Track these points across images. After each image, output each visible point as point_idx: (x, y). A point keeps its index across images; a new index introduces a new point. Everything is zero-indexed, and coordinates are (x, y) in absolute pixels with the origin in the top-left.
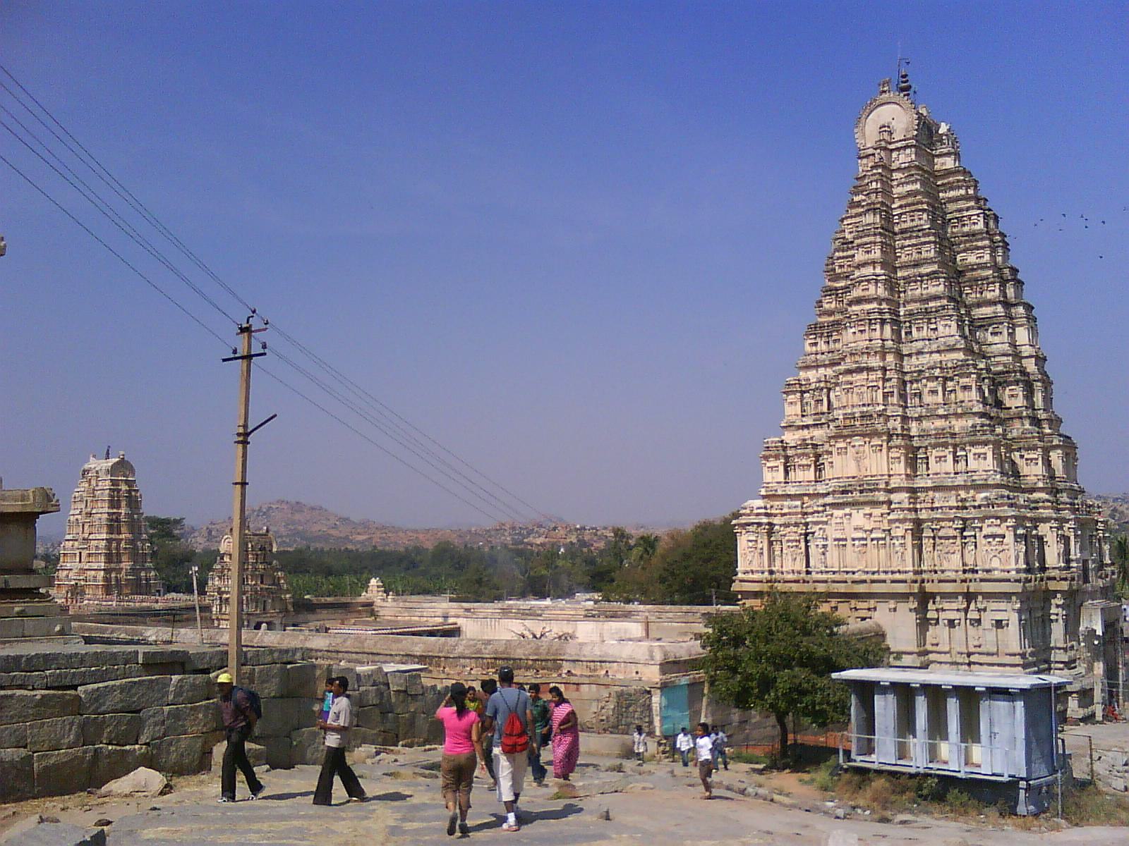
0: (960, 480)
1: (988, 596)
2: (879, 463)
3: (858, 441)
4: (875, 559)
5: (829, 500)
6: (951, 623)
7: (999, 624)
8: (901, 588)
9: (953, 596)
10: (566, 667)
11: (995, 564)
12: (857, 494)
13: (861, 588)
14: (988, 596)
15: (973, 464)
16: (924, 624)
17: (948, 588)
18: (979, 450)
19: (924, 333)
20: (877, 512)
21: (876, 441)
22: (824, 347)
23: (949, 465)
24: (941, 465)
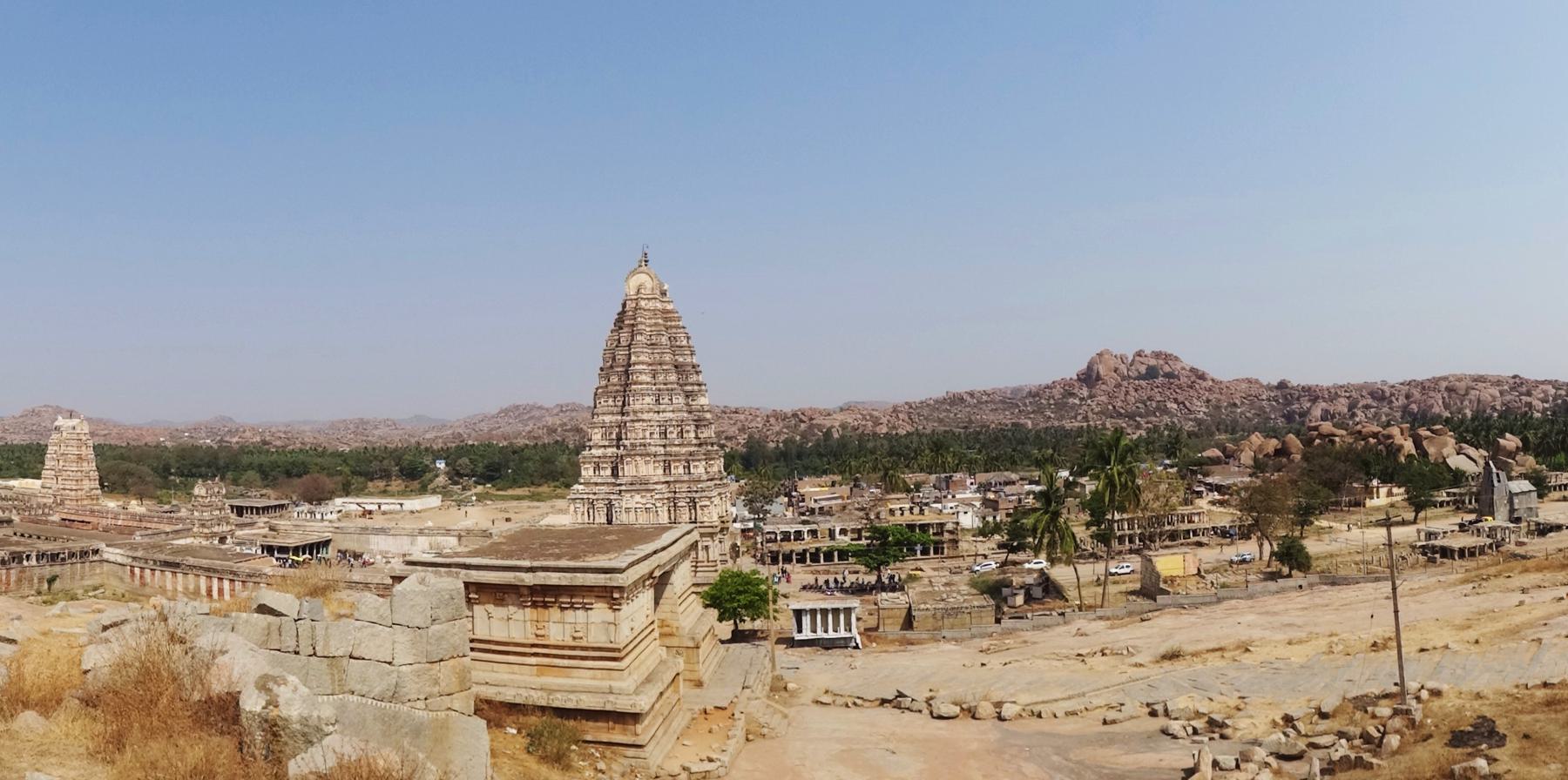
12: (640, 486)
24: (678, 470)
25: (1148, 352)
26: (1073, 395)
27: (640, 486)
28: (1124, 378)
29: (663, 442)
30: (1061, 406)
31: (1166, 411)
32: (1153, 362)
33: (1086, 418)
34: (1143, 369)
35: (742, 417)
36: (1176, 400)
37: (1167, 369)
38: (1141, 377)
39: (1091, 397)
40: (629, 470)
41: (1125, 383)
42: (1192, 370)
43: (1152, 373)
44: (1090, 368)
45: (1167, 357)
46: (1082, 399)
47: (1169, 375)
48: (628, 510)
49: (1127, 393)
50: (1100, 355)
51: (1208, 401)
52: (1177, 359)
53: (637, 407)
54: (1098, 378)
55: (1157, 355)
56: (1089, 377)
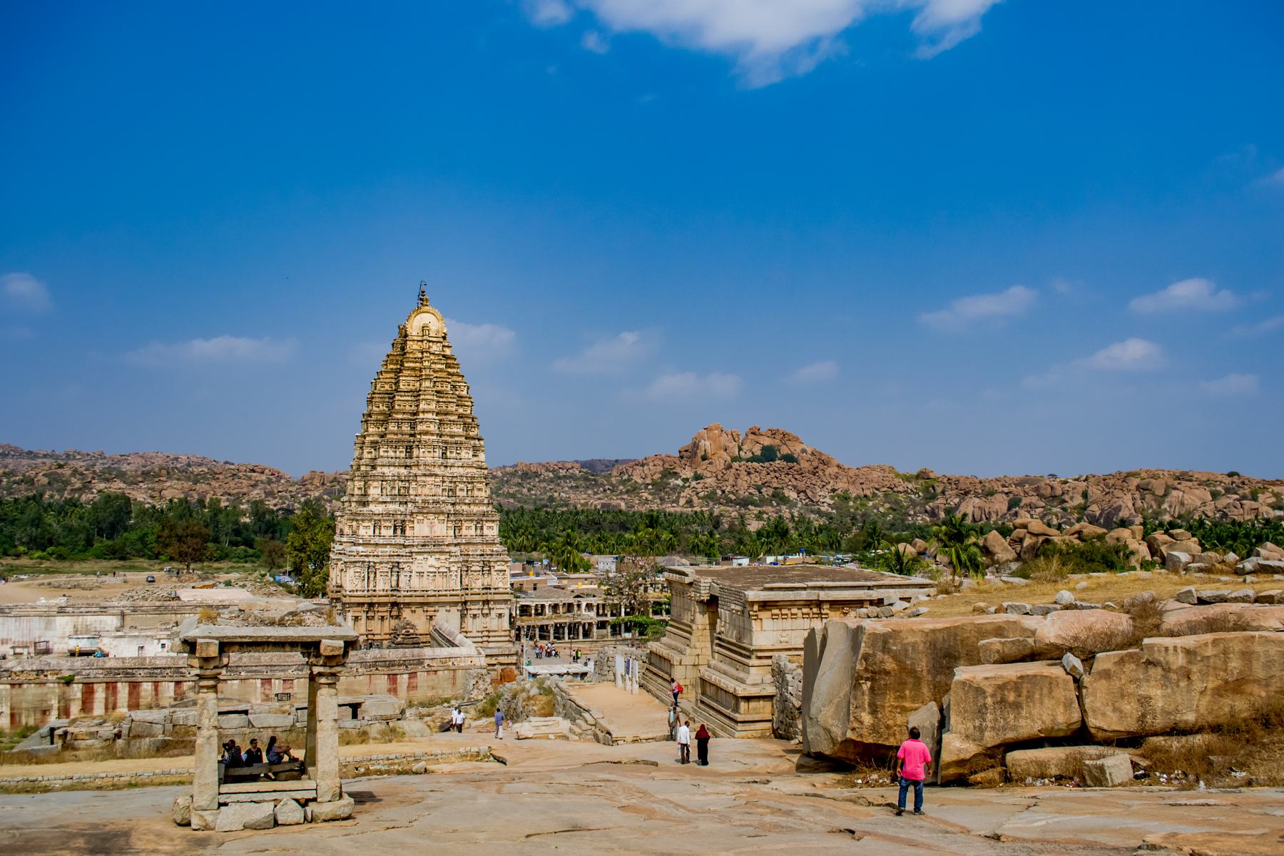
0: (479, 540)
1: (496, 602)
2: (442, 529)
3: (431, 517)
4: (440, 583)
5: (415, 549)
6: (475, 616)
7: (500, 615)
9: (477, 602)
10: (427, 662)
11: (500, 585)
13: (432, 600)
14: (496, 602)
15: (486, 531)
16: (463, 616)
17: (477, 597)
18: (490, 524)
19: (454, 455)
20: (443, 557)
21: (442, 517)
22: (391, 454)
23: (472, 532)
24: (469, 531)
26: (676, 475)
27: (432, 546)
28: (734, 459)
29: (452, 500)
30: (659, 487)
31: (783, 500)
32: (767, 442)
33: (690, 502)
35: (264, 477)
37: (785, 450)
39: (698, 477)
40: (420, 529)
41: (736, 465)
43: (768, 454)
44: (696, 445)
46: (685, 480)
47: (789, 458)
48: (420, 574)
52: (796, 439)
53: (429, 460)
55: (774, 434)
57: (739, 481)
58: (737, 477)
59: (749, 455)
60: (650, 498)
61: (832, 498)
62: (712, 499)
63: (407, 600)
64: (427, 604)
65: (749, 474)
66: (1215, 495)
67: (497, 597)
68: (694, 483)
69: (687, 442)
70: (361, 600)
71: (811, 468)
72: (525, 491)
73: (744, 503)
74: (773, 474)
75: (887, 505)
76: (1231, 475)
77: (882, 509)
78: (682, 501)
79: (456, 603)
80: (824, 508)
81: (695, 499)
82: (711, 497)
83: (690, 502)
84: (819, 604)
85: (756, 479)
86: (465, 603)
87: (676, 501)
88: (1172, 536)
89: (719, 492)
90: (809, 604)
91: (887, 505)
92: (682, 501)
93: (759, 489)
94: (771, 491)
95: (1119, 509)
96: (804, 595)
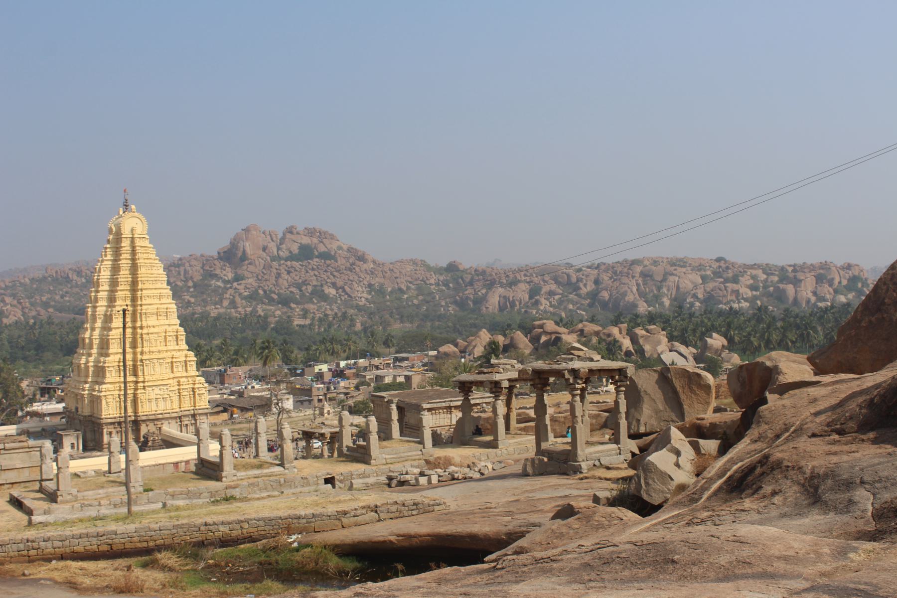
8: (175, 415)
13: (160, 416)
17: (187, 413)
25: (300, 228)
28: (273, 259)
31: (324, 297)
32: (306, 240)
33: (233, 304)
34: (295, 249)
36: (334, 285)
37: (322, 248)
38: (292, 257)
41: (275, 264)
42: (350, 250)
43: (306, 253)
44: (234, 245)
45: (323, 235)
46: (226, 282)
48: (150, 400)
49: (278, 276)
50: (247, 230)
51: (370, 285)
52: (332, 237)
54: (244, 257)
55: (311, 232)
56: (232, 255)
57: (280, 280)
58: (278, 276)
59: (287, 254)
60: (192, 300)
61: (369, 293)
62: (255, 299)
63: (144, 418)
64: (157, 420)
65: (289, 273)
66: (704, 278)
67: (200, 412)
68: (235, 284)
69: (225, 243)
70: (113, 421)
71: (348, 265)
72: (58, 297)
73: (285, 302)
74: (312, 273)
75: (420, 298)
76: (719, 260)
77: (416, 302)
78: (226, 303)
79: (175, 418)
80: (363, 302)
81: (238, 299)
82: (253, 297)
83: (233, 304)
84: (450, 408)
85: (297, 277)
86: (180, 418)
87: (220, 302)
88: (647, 331)
89: (261, 292)
90: (446, 408)
91: (420, 298)
92: (226, 303)
93: (299, 286)
94: (310, 289)
95: (624, 294)
96: (444, 405)
